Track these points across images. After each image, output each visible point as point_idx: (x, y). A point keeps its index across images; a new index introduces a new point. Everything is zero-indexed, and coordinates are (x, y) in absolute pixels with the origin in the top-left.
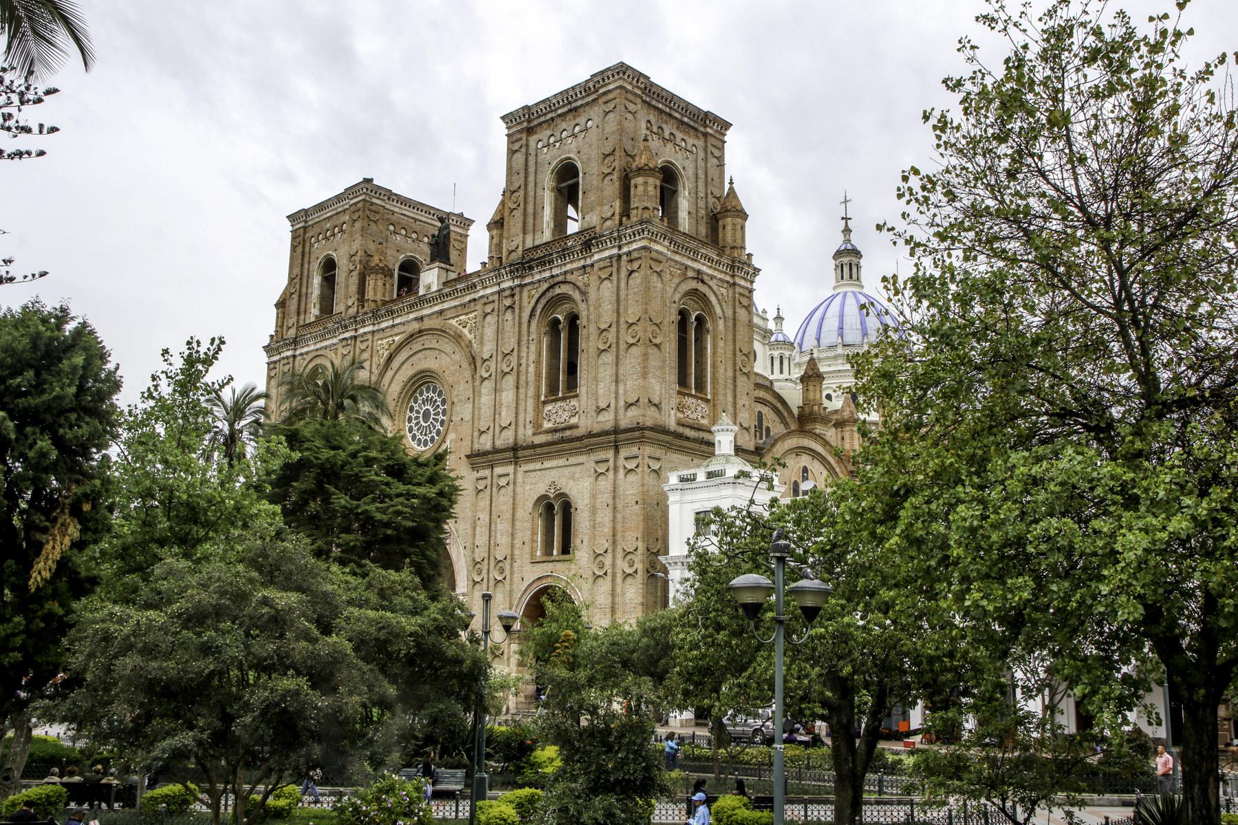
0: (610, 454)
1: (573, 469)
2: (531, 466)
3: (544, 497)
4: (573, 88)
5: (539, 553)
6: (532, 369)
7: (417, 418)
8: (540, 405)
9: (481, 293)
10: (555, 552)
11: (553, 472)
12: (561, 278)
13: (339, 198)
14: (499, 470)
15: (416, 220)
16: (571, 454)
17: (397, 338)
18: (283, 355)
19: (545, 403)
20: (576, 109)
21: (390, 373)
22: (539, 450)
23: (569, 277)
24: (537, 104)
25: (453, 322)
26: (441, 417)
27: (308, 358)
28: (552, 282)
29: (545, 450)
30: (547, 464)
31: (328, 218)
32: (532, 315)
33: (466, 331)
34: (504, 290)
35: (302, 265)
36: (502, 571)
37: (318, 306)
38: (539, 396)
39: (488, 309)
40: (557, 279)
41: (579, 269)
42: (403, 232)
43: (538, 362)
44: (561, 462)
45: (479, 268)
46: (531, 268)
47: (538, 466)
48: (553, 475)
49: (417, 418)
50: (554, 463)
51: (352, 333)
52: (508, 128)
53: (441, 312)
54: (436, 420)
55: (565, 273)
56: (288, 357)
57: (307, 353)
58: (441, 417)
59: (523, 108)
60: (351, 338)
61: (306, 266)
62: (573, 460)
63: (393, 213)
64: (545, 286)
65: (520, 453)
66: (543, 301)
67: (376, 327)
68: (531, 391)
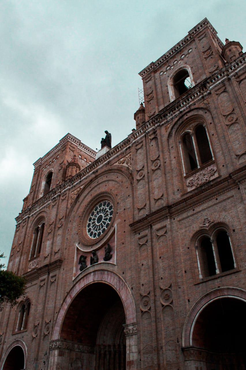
1: (224, 204)
2: (180, 218)
3: (201, 231)
4: (178, 44)
5: (201, 277)
6: (174, 162)
7: (94, 219)
8: (182, 179)
10: (218, 271)
11: (204, 213)
14: (156, 227)
15: (91, 157)
19: (186, 178)
21: (78, 204)
22: (189, 202)
23: (192, 107)
24: (158, 60)
25: (117, 164)
26: (108, 222)
27: (35, 216)
28: (181, 115)
29: (195, 199)
30: (197, 209)
32: (170, 135)
33: (125, 165)
34: (149, 132)
35: (37, 180)
36: (167, 298)
37: (43, 194)
38: (181, 174)
40: (183, 113)
42: (85, 160)
43: (178, 157)
44: (210, 203)
45: (132, 132)
47: (191, 213)
48: (206, 214)
49: (94, 219)
50: (205, 206)
52: (142, 77)
53: (109, 163)
54: (105, 223)
55: (189, 107)
58: (108, 222)
59: (151, 64)
61: (39, 180)
62: (221, 198)
63: (81, 151)
65: (173, 210)
66: (176, 127)
68: (176, 173)
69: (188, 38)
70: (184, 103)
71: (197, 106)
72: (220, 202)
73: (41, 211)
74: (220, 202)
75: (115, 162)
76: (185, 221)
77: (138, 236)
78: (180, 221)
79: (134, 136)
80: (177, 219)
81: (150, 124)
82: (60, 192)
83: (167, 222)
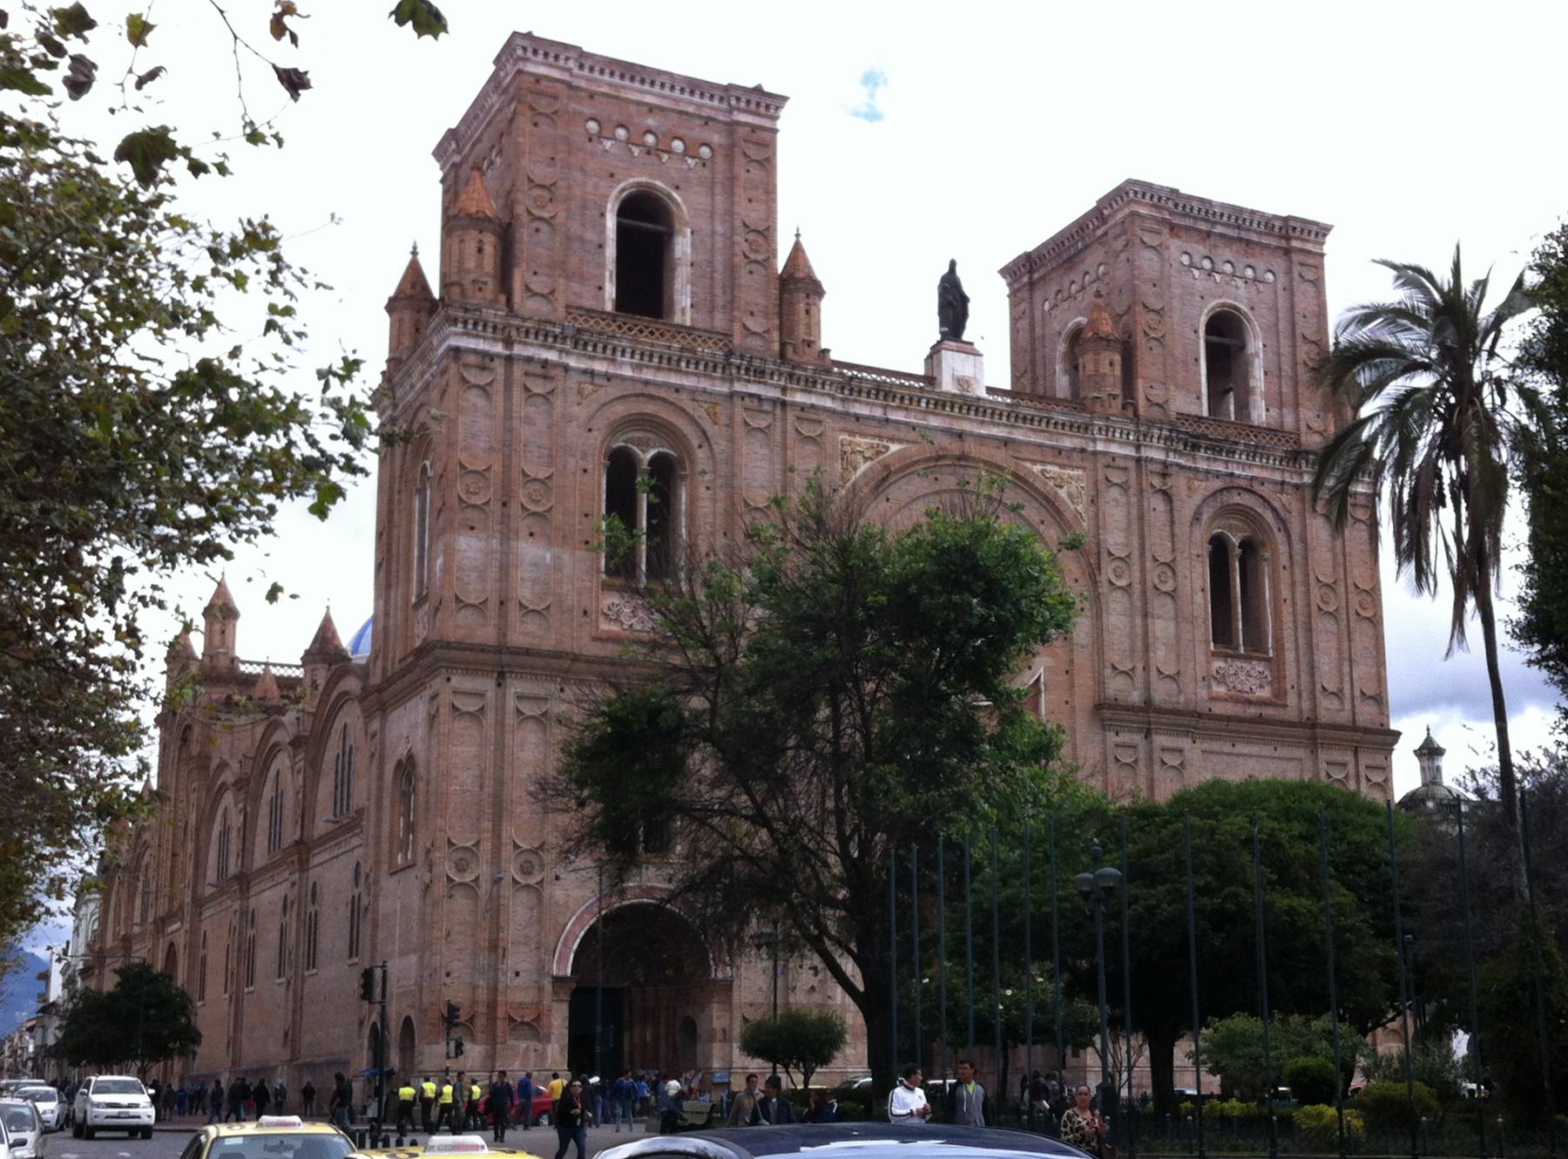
0: (1349, 757)
4: (1253, 212)
9: (1100, 447)
11: (1251, 763)
12: (1243, 483)
13: (695, 86)
14: (1161, 740)
16: (1284, 744)
17: (894, 448)
18: (518, 350)
20: (1248, 242)
23: (1257, 487)
24: (1190, 198)
25: (1037, 468)
27: (613, 391)
29: (1245, 727)
30: (1242, 748)
31: (652, 109)
33: (1063, 493)
39: (1116, 477)
41: (1275, 482)
44: (1266, 750)
46: (1196, 447)
47: (1227, 748)
51: (774, 393)
55: (1252, 478)
56: (545, 363)
57: (609, 377)
60: (774, 401)
64: (1218, 484)
67: (838, 406)
69: (1278, 224)
70: (1244, 457)
71: (1265, 490)
72: (1279, 758)
73: (653, 391)
74: (1279, 758)
75: (1027, 456)
76: (1215, 758)
77: (1112, 738)
78: (1203, 752)
79: (1107, 431)
80: (1206, 746)
81: (1159, 438)
82: (784, 390)
83: (1185, 743)
